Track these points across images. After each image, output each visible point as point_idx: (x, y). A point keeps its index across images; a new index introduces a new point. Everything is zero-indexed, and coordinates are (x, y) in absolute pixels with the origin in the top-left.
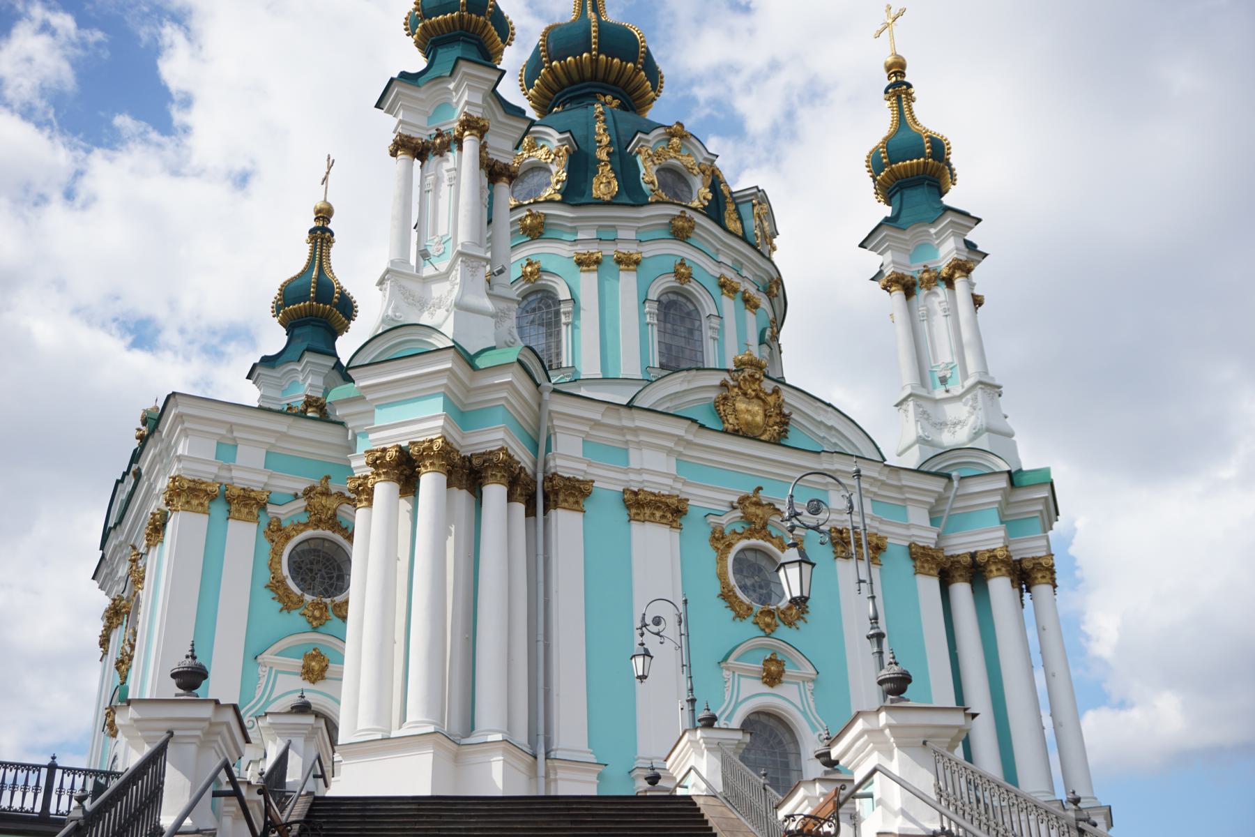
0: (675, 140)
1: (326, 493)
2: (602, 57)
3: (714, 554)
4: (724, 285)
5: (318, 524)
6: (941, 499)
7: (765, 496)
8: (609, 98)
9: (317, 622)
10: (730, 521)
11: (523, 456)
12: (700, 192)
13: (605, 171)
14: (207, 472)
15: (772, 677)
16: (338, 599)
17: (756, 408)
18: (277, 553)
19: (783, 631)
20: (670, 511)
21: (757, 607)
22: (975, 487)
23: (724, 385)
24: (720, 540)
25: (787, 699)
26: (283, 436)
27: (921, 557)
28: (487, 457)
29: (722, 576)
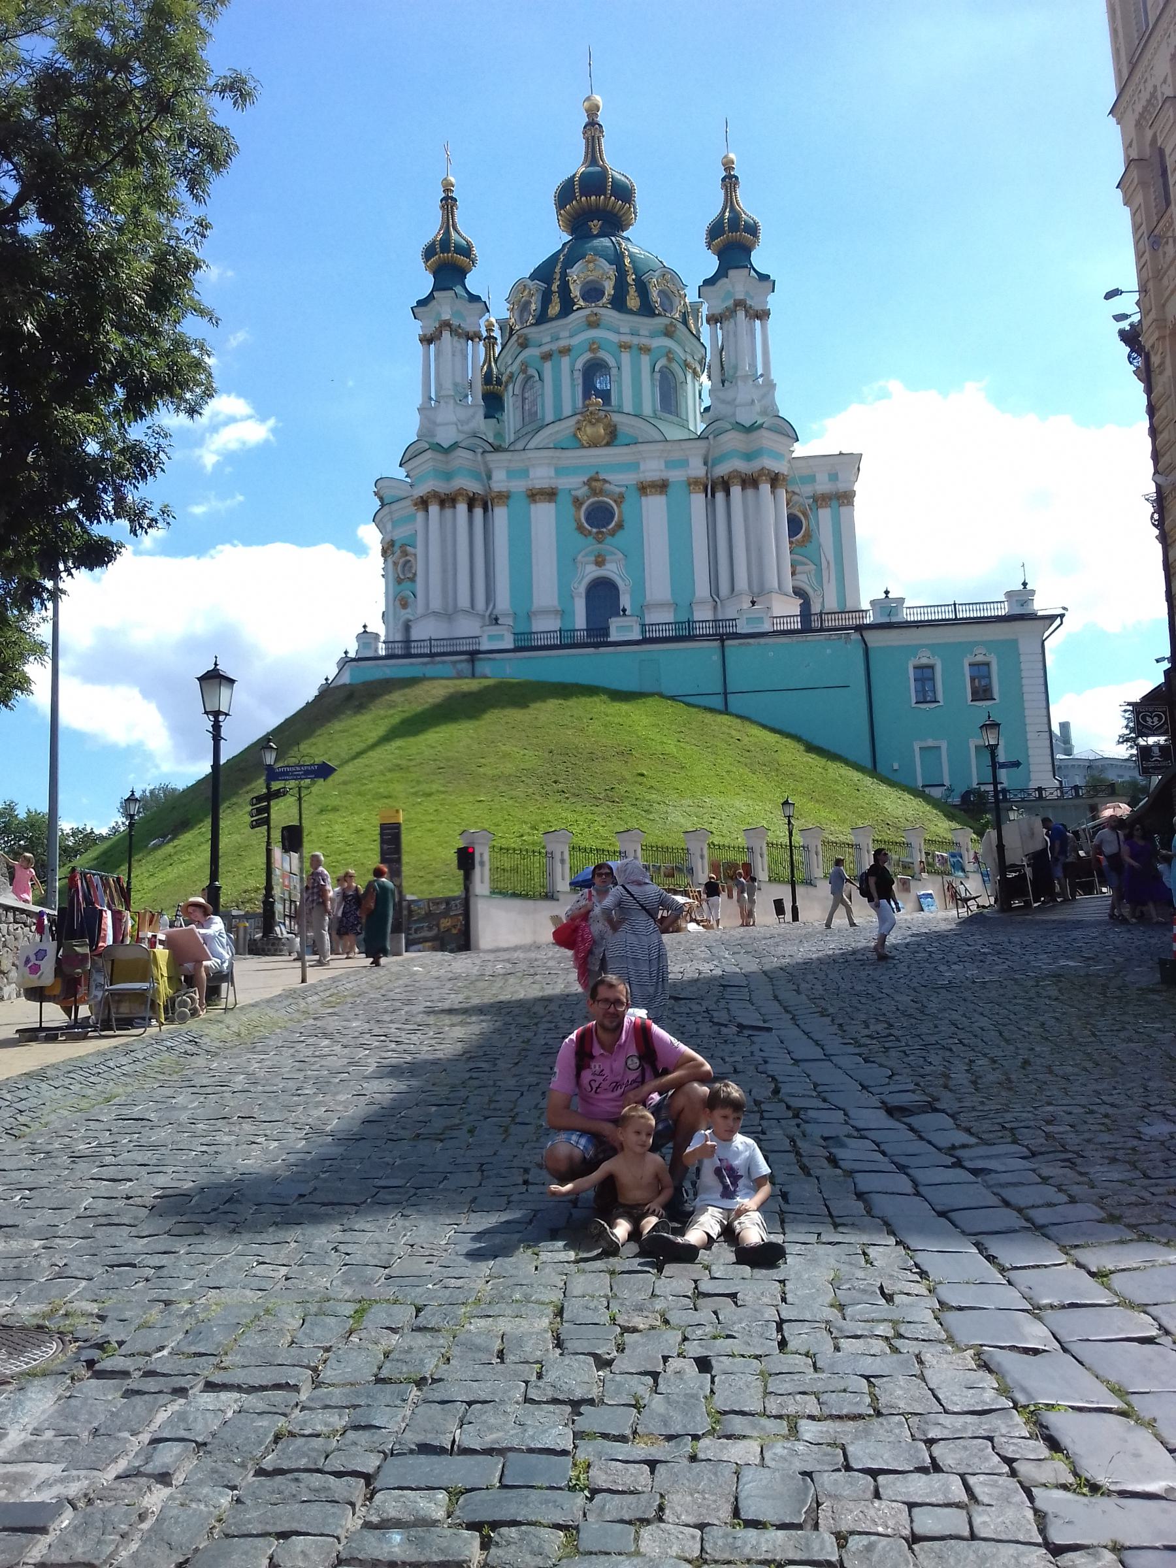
0: (591, 265)
2: (583, 199)
3: (572, 510)
8: (595, 222)
10: (582, 492)
11: (474, 486)
13: (556, 298)
15: (600, 562)
20: (551, 494)
21: (594, 530)
22: (724, 438)
23: (578, 422)
24: (577, 502)
25: (611, 570)
27: (693, 484)
29: (578, 521)
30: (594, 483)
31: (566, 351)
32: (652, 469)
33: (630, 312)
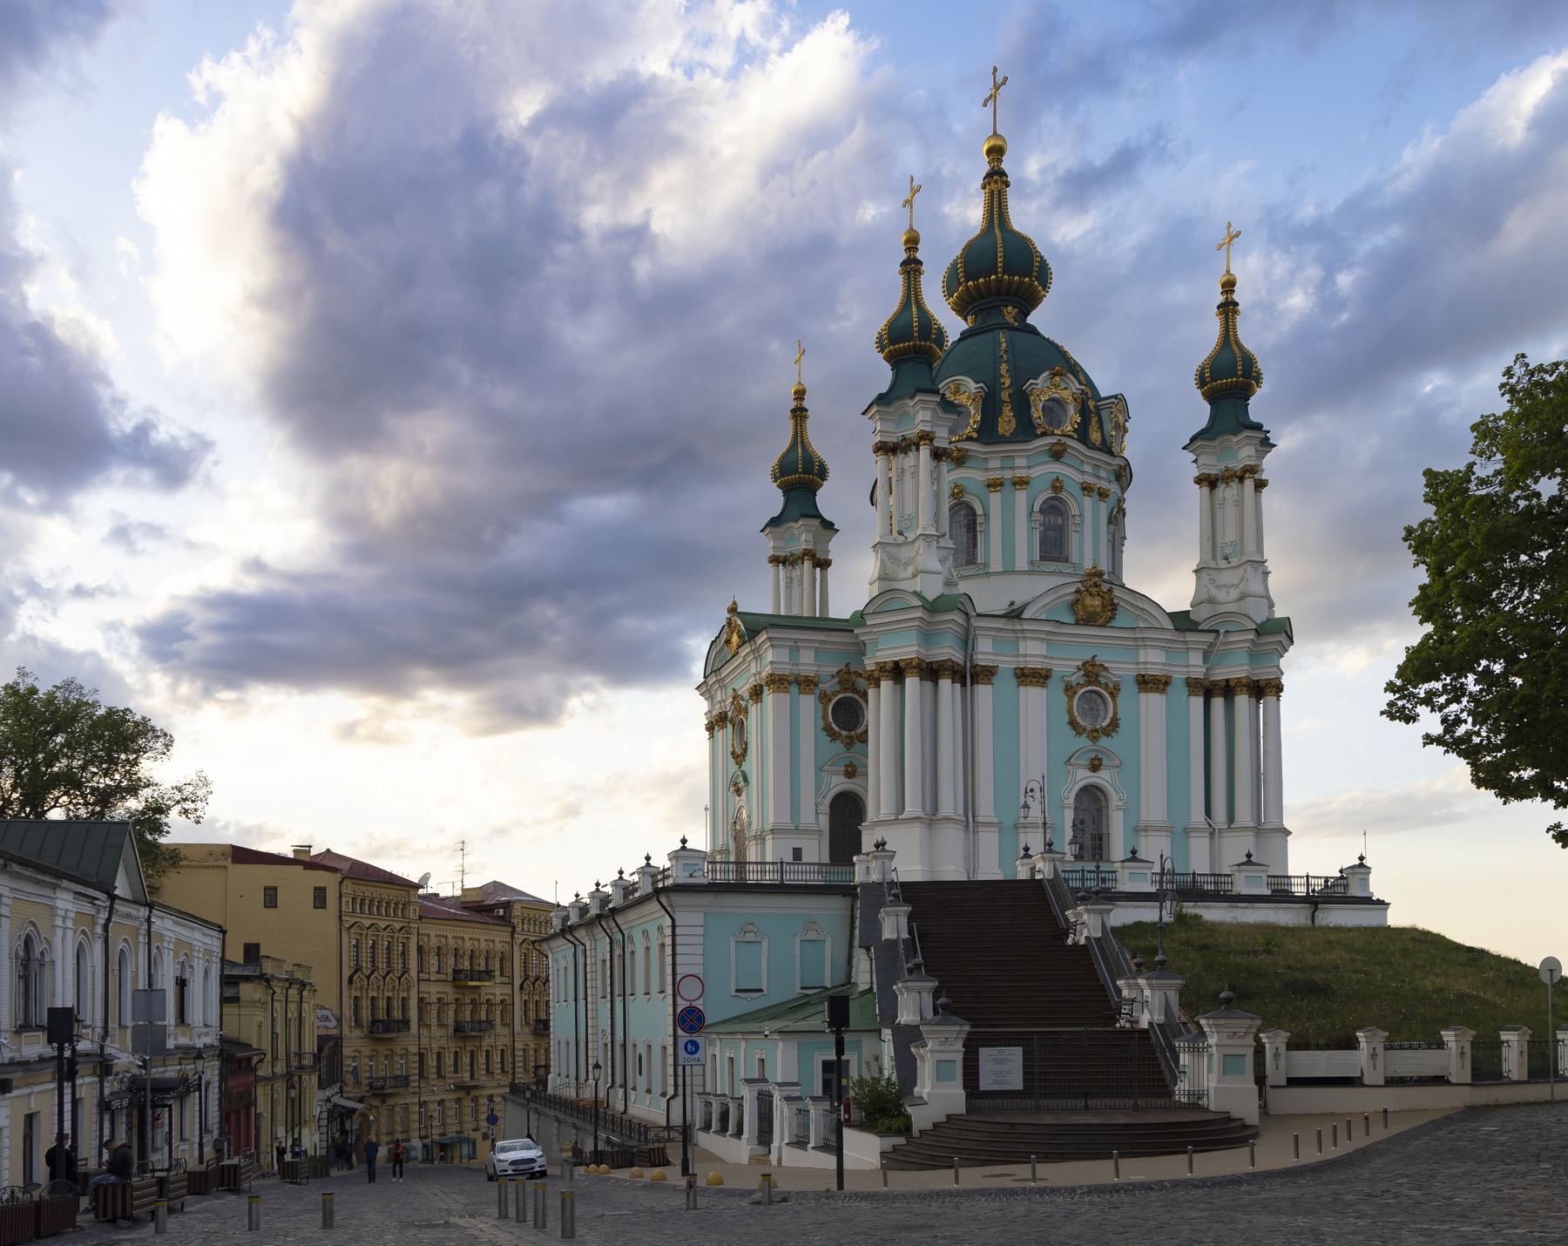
1: (849, 672)
4: (1086, 489)
5: (846, 690)
6: (1211, 645)
7: (1098, 660)
9: (849, 743)
10: (1077, 678)
12: (1073, 415)
14: (786, 670)
15: (1095, 766)
16: (859, 731)
17: (1097, 602)
18: (825, 710)
19: (1104, 741)
24: (1070, 690)
26: (823, 642)
27: (1193, 685)
28: (942, 664)
29: (1070, 712)
30: (1092, 671)
31: (1021, 483)
32: (1153, 660)
33: (1093, 447)
